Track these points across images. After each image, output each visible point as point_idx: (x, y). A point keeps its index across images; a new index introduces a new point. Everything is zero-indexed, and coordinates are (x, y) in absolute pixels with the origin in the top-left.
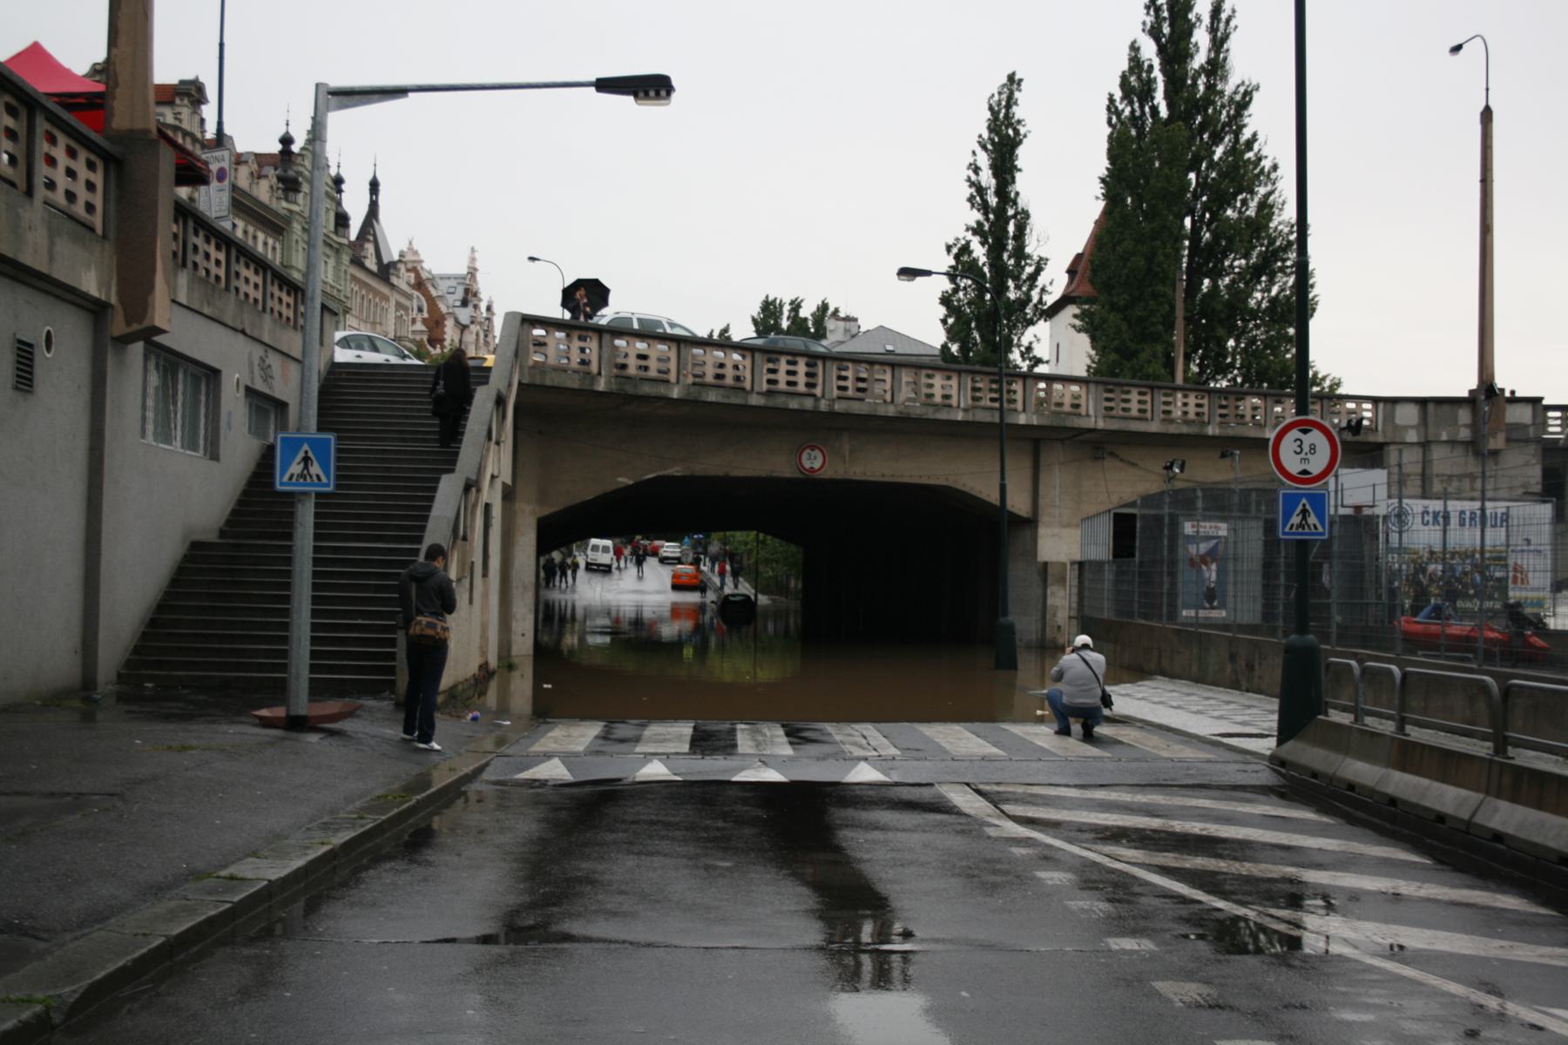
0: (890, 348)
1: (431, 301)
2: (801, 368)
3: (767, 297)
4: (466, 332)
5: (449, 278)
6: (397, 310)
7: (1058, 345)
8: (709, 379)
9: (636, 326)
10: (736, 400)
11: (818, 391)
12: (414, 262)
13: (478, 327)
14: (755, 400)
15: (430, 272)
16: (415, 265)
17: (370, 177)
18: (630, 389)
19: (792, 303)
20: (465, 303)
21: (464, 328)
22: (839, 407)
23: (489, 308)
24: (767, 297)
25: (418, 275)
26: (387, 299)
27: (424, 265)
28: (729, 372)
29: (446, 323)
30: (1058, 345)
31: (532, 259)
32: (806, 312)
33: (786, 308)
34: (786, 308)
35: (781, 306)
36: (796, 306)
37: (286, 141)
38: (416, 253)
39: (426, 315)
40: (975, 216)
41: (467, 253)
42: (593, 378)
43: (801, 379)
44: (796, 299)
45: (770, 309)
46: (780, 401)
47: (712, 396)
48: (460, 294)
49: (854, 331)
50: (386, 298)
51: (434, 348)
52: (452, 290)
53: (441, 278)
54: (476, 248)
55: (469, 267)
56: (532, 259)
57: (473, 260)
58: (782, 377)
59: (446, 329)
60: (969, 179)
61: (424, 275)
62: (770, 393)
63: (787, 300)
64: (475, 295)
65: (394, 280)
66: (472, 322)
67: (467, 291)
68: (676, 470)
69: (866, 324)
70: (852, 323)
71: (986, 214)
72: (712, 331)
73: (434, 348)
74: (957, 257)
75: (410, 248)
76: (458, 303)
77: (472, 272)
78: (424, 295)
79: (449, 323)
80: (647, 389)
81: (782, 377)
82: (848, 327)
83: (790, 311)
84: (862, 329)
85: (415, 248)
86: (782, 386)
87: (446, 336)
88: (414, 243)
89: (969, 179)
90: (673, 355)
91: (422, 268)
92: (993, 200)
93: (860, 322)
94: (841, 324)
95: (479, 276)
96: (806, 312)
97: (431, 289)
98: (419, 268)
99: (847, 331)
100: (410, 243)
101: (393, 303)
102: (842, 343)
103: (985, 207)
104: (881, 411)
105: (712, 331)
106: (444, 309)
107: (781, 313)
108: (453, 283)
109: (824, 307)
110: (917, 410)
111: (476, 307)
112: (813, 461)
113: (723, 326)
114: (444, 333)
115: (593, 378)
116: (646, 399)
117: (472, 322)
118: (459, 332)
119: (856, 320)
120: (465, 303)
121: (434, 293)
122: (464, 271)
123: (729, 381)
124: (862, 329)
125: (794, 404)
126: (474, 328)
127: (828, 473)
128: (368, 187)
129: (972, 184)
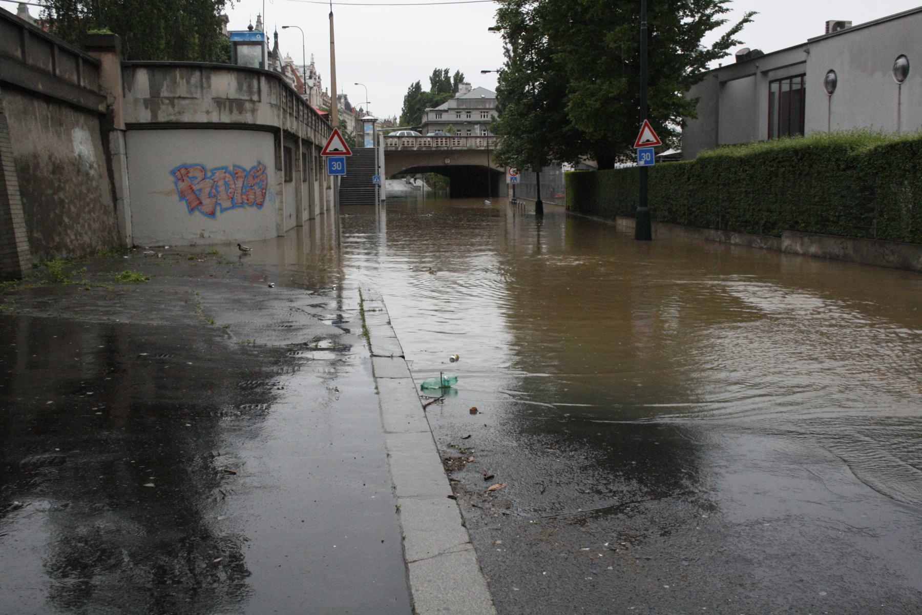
0: (483, 96)
2: (444, 140)
4: (312, 90)
8: (423, 145)
9: (406, 135)
10: (429, 149)
11: (448, 145)
14: (433, 149)
17: (274, 31)
18: (406, 149)
19: (445, 71)
20: (310, 77)
22: (454, 148)
23: (319, 78)
28: (427, 143)
31: (356, 84)
32: (451, 74)
33: (443, 73)
34: (443, 73)
35: (441, 72)
36: (447, 72)
37: (250, 28)
38: (290, 58)
39: (296, 84)
40: (506, 60)
42: (397, 148)
43: (444, 143)
45: (437, 73)
46: (439, 148)
47: (424, 149)
49: (469, 89)
56: (356, 84)
57: (313, 59)
58: (439, 143)
60: (504, 47)
61: (294, 67)
62: (437, 147)
63: (443, 70)
64: (315, 74)
65: (287, 74)
67: (311, 72)
68: (415, 166)
69: (474, 86)
71: (510, 59)
74: (500, 75)
75: (288, 56)
77: (312, 64)
80: (409, 149)
81: (439, 143)
84: (473, 88)
86: (440, 145)
89: (504, 47)
90: (414, 140)
92: (512, 54)
93: (471, 85)
94: (464, 86)
95: (315, 65)
96: (451, 74)
97: (297, 73)
99: (467, 89)
102: (465, 94)
103: (509, 56)
104: (464, 148)
107: (441, 75)
109: (458, 73)
110: (474, 147)
111: (315, 79)
112: (448, 161)
113: (417, 81)
115: (397, 148)
116: (409, 151)
119: (470, 84)
120: (310, 77)
123: (427, 145)
124: (473, 88)
125: (442, 149)
126: (315, 88)
127: (452, 164)
128: (273, 35)
129: (505, 48)
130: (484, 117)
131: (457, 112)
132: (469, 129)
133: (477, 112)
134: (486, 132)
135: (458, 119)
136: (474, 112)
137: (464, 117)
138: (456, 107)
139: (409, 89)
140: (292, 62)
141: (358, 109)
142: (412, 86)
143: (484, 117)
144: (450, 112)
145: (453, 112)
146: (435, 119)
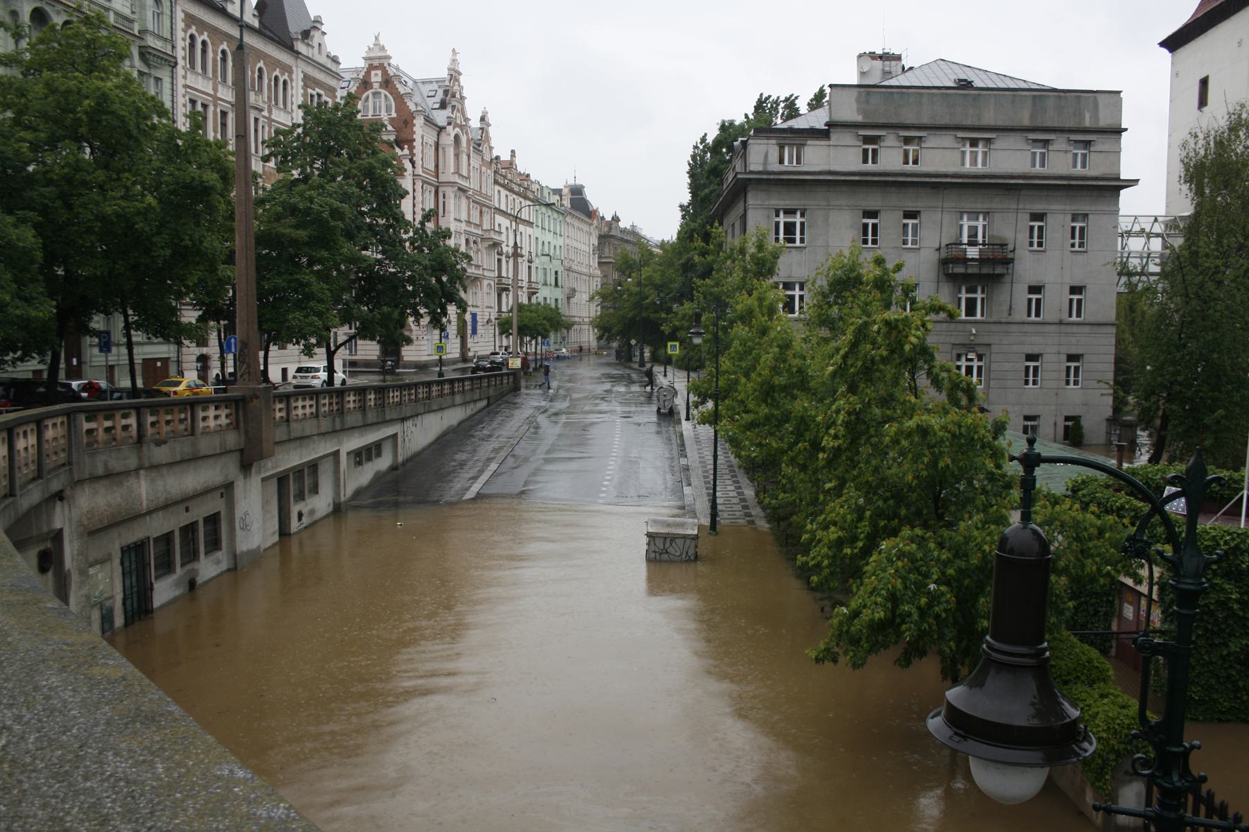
1: (400, 99)
3: (761, 94)
4: (443, 134)
5: (431, 82)
6: (305, 86)
7: (1204, 83)
12: (380, 58)
13: (457, 129)
15: (398, 69)
16: (381, 61)
19: (787, 100)
20: (443, 105)
21: (441, 129)
24: (761, 94)
25: (385, 72)
26: (288, 69)
27: (392, 61)
29: (415, 121)
30: (1204, 83)
38: (382, 49)
39: (394, 115)
41: (448, 56)
44: (792, 95)
48: (440, 95)
50: (288, 69)
51: (402, 149)
52: (433, 93)
53: (423, 83)
54: (457, 51)
55: (449, 69)
59: (415, 129)
61: (391, 72)
66: (449, 124)
67: (446, 92)
70: (894, 63)
72: (706, 134)
73: (402, 149)
76: (437, 106)
77: (454, 75)
78: (391, 94)
79: (419, 122)
82: (887, 69)
83: (785, 108)
85: (382, 43)
87: (415, 136)
88: (380, 38)
91: (389, 65)
98: (386, 65)
100: (377, 38)
101: (298, 77)
105: (706, 134)
106: (412, 108)
108: (435, 86)
114: (414, 133)
117: (449, 124)
118: (435, 134)
120: (443, 105)
121: (402, 90)
122: (444, 74)
130: (974, 162)
131: (868, 140)
132: (911, 205)
133: (947, 140)
134: (980, 223)
135: (870, 166)
136: (933, 140)
137: (891, 159)
138: (859, 118)
139: (696, 147)
140: (389, 58)
141: (608, 218)
142: (703, 140)
143: (974, 162)
144: (836, 137)
145: (846, 138)
146: (774, 166)
